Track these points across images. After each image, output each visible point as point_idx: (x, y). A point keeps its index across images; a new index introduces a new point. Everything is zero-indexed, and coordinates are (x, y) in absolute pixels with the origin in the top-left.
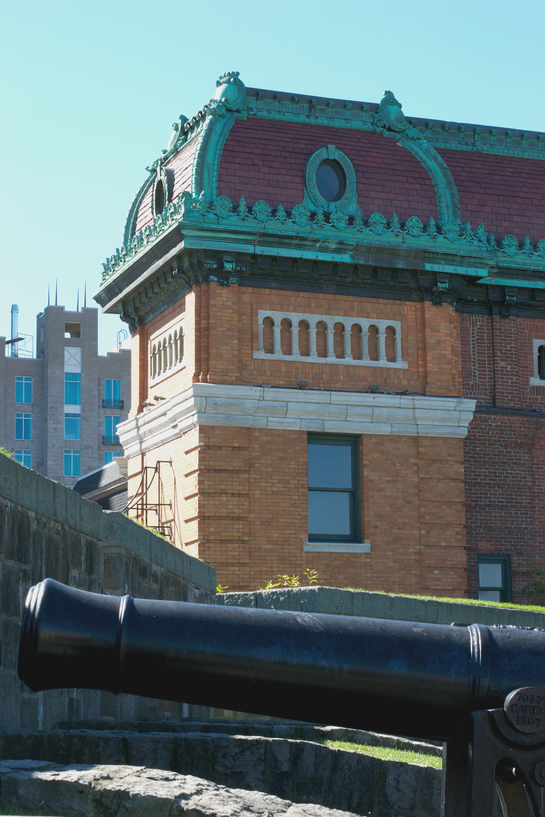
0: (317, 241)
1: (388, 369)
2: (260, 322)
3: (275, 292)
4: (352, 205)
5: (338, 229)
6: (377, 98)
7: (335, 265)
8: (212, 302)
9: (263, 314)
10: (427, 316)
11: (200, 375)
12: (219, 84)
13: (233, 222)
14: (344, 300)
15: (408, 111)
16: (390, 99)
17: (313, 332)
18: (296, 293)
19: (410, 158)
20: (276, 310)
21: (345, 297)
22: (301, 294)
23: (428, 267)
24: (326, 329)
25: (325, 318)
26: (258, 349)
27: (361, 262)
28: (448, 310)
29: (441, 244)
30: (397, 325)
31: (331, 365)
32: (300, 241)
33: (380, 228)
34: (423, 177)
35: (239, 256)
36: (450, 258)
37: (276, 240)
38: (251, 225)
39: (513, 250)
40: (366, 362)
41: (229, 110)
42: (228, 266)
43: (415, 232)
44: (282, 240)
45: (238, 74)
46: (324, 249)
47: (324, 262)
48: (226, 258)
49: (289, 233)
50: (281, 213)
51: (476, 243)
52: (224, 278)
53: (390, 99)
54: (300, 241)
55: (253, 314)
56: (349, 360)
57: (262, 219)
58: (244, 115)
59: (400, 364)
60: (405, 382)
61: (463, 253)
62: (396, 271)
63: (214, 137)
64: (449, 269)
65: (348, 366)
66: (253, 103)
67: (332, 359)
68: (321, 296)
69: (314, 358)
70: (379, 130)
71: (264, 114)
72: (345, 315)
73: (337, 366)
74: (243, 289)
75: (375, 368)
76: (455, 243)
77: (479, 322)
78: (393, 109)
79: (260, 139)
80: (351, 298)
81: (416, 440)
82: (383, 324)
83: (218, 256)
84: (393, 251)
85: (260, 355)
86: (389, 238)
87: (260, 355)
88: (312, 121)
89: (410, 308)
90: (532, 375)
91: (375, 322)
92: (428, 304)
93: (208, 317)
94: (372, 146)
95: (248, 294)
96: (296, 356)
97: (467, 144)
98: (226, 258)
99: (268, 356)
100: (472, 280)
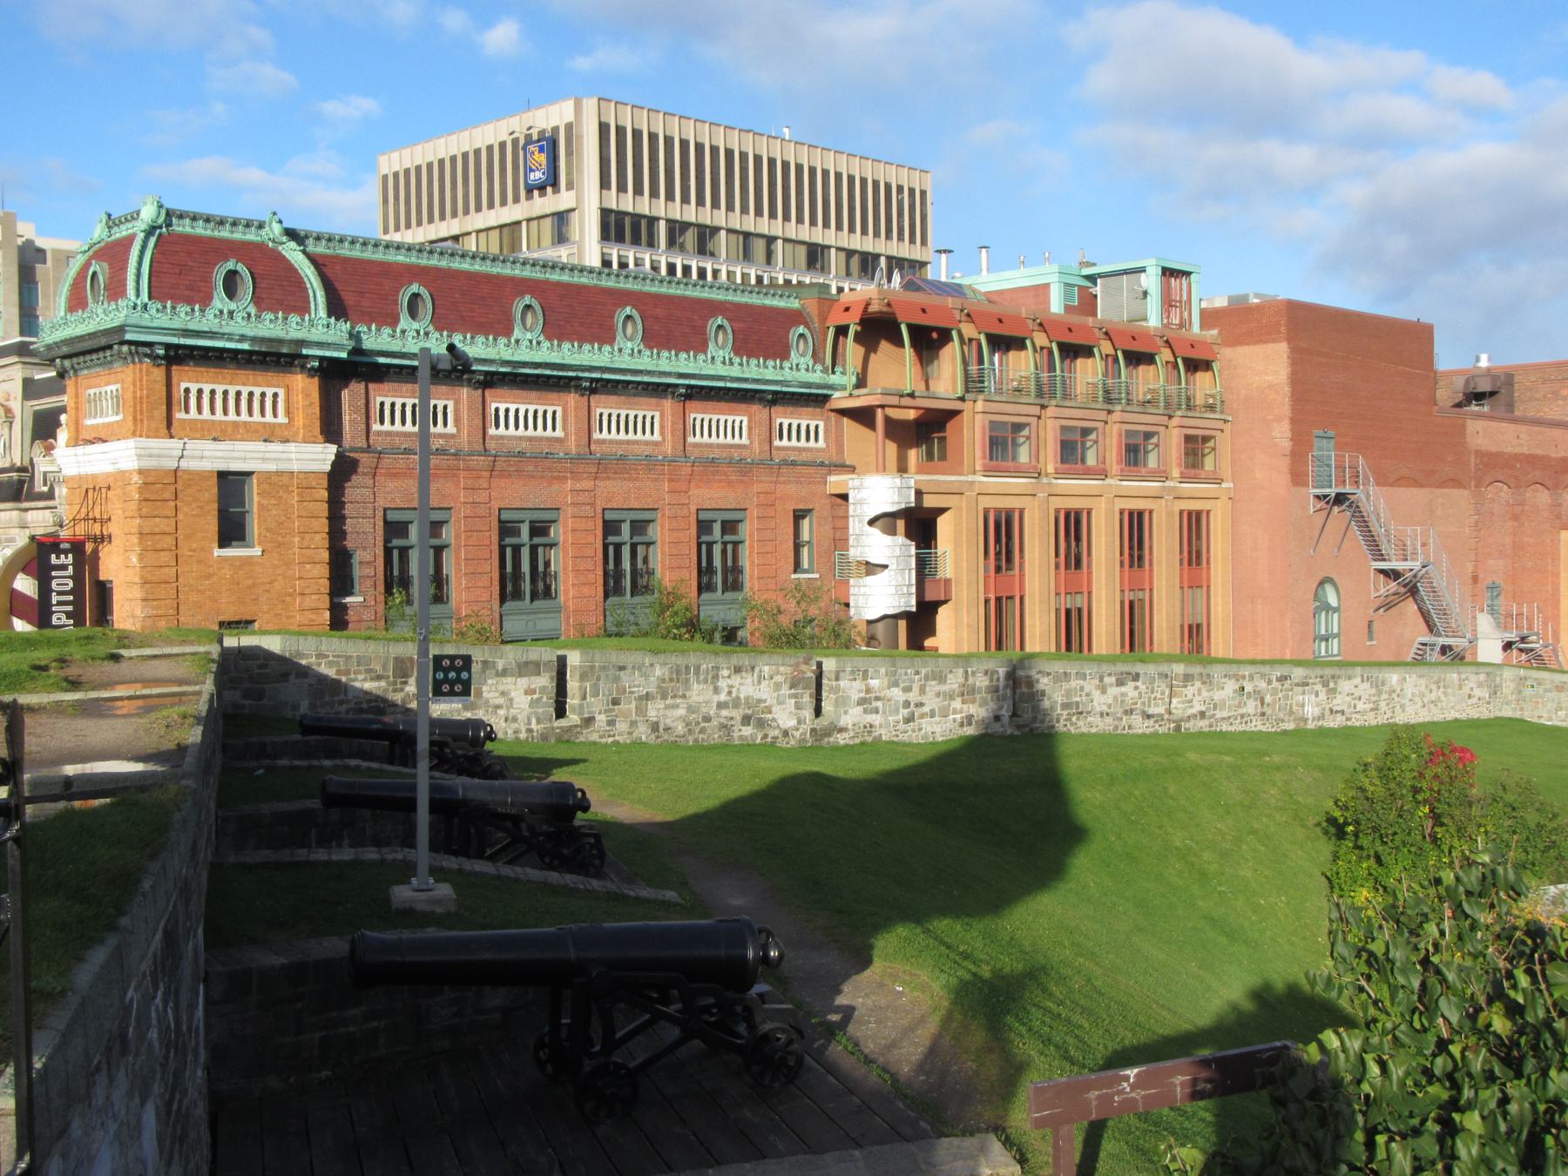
9: (184, 385)
23: (305, 352)
35: (168, 346)
36: (320, 345)
38: (177, 324)
46: (230, 340)
84: (280, 341)
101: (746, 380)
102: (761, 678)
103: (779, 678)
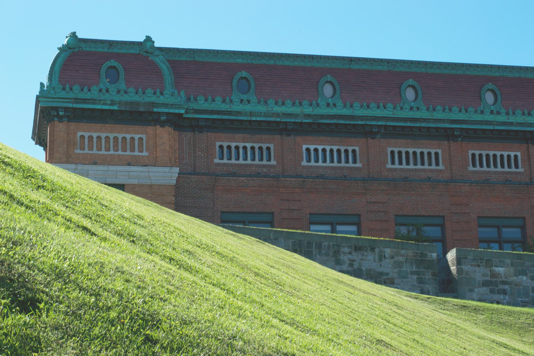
0: (101, 100)
1: (139, 156)
2: (78, 137)
3: (85, 124)
4: (122, 85)
6: (141, 39)
7: (112, 111)
8: (55, 129)
9: (79, 134)
10: (157, 132)
12: (67, 37)
13: (63, 94)
15: (156, 45)
16: (148, 39)
17: (103, 141)
18: (96, 124)
19: (153, 63)
20: (85, 132)
21: (119, 125)
22: (98, 125)
23: (155, 110)
24: (110, 139)
25: (109, 135)
26: (77, 149)
27: (123, 109)
28: (168, 129)
29: (162, 99)
30: (144, 137)
31: (111, 155)
32: (93, 101)
34: (158, 72)
35: (66, 109)
36: (166, 105)
38: (71, 95)
39: (202, 102)
41: (70, 48)
42: (61, 113)
43: (149, 95)
44: (85, 101)
45: (75, 33)
46: (105, 104)
47: (105, 110)
48: (60, 110)
49: (88, 98)
50: (86, 89)
51: (179, 99)
52: (60, 119)
53: (148, 39)
57: (77, 92)
58: (76, 50)
59: (145, 154)
60: (147, 161)
61: (171, 103)
62: (141, 113)
63: (60, 60)
64: (166, 110)
65: (119, 155)
66: (83, 45)
67: (112, 152)
68: (108, 125)
70: (142, 53)
71: (88, 49)
72: (119, 133)
73: (114, 155)
74: (71, 123)
75: (132, 155)
76: (170, 99)
77: (188, 135)
78: (149, 44)
79: (80, 60)
80: (122, 126)
81: (151, 186)
82: (137, 137)
83: (56, 109)
84: (138, 104)
85: (78, 151)
86: (137, 98)
87: (78, 151)
88: (110, 51)
89: (150, 129)
90: (215, 158)
91: (133, 136)
92: (158, 127)
94: (137, 60)
97: (190, 57)
98: (60, 110)
99: (82, 152)
100: (180, 115)
101: (511, 124)
102: (382, 257)
103: (401, 259)
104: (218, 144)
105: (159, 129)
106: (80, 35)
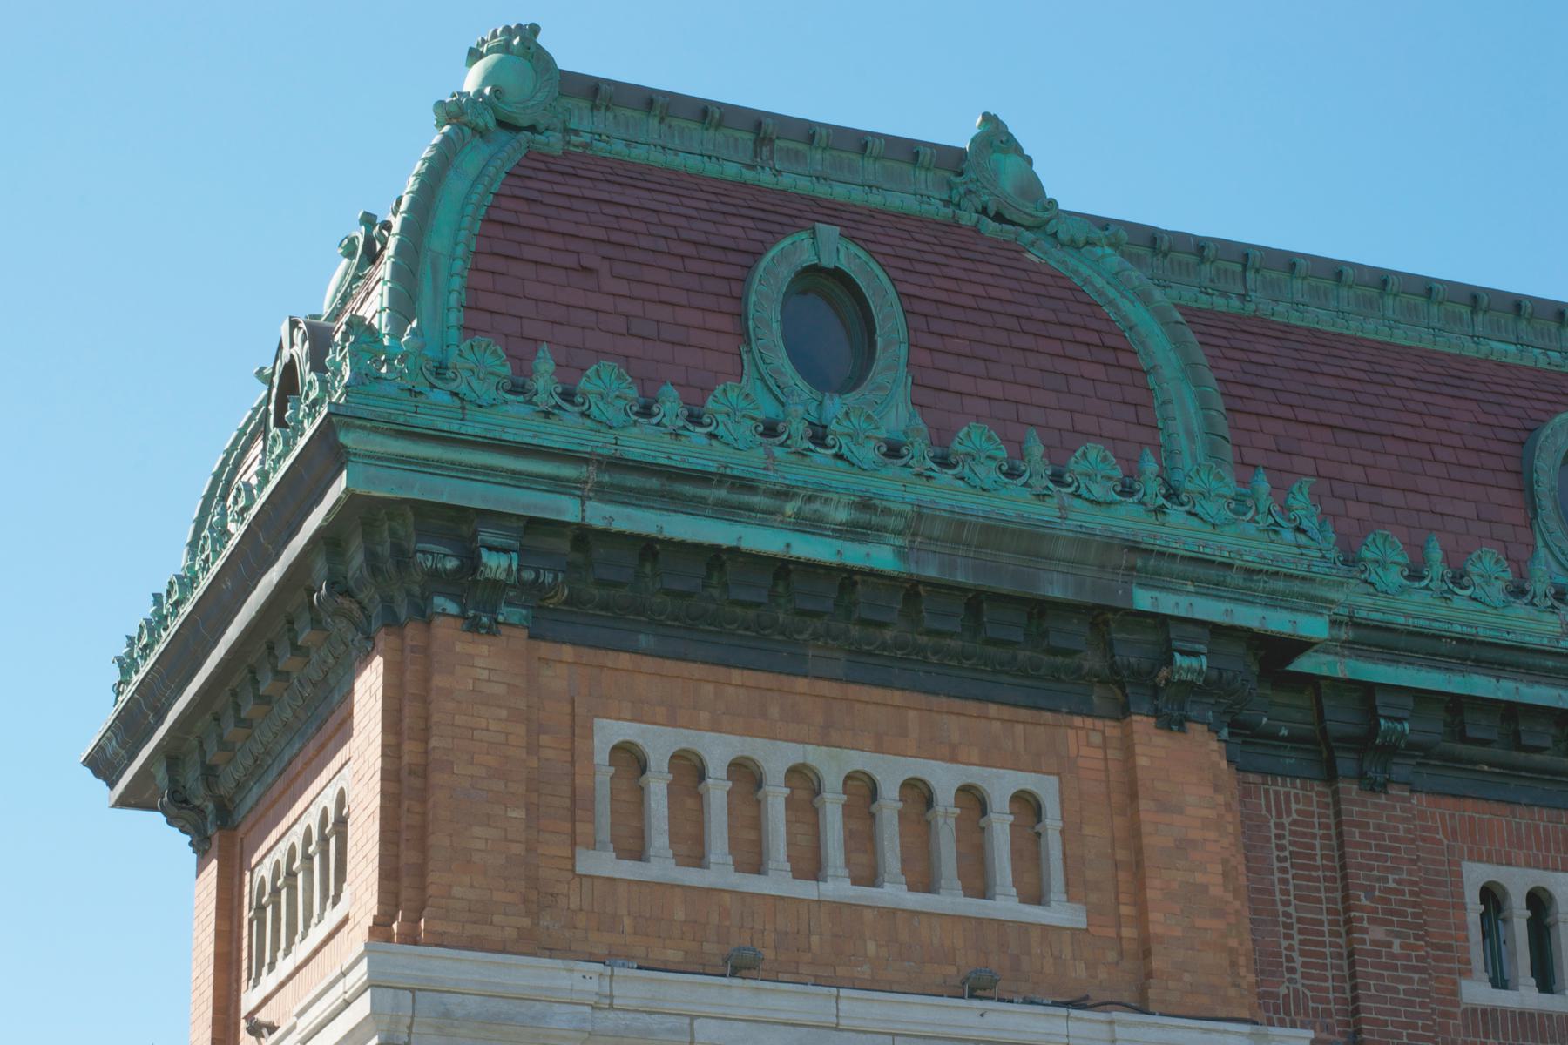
0: (785, 494)
1: (1024, 927)
2: (602, 756)
3: (649, 663)
5: (854, 470)
6: (960, 133)
7: (846, 578)
8: (438, 681)
9: (610, 732)
10: (1142, 761)
11: (394, 919)
12: (474, 55)
13: (515, 420)
14: (875, 703)
16: (996, 137)
17: (776, 796)
18: (720, 673)
19: (1071, 292)
20: (653, 719)
21: (877, 694)
22: (737, 676)
23: (1143, 600)
24: (817, 792)
25: (814, 756)
26: (593, 845)
27: (931, 572)
29: (1178, 531)
30: (1046, 788)
31: (838, 908)
32: (735, 493)
33: (986, 473)
36: (1211, 572)
37: (654, 483)
38: (566, 431)
39: (1394, 577)
40: (951, 900)
41: (503, 124)
42: (496, 564)
43: (1098, 491)
45: (535, 29)
46: (812, 525)
47: (810, 568)
48: (487, 536)
49: (698, 464)
50: (670, 404)
51: (1288, 535)
52: (480, 602)
53: (996, 137)
54: (735, 493)
55: (577, 732)
56: (894, 893)
57: (607, 413)
58: (553, 142)
59: (1061, 913)
60: (1080, 971)
61: (1250, 560)
62: (1040, 609)
63: (454, 187)
65: (891, 913)
66: (584, 120)
67: (837, 887)
68: (801, 684)
69: (778, 882)
70: (967, 218)
72: (878, 749)
73: (856, 908)
74: (545, 649)
75: (980, 921)
76: (1225, 538)
77: (1297, 801)
78: (1010, 163)
80: (896, 697)
82: (1001, 785)
83: (457, 525)
84: (1030, 542)
85: (600, 863)
86: (1015, 504)
87: (600, 863)
88: (766, 178)
89: (1086, 738)
90: (1467, 973)
91: (976, 775)
92: (1141, 724)
93: (425, 734)
94: (950, 261)
95: (562, 667)
96: (720, 873)
97: (1224, 294)
98: (487, 536)
99: (627, 870)
104: (1476, 875)
105: (1151, 744)
106: (573, 54)
